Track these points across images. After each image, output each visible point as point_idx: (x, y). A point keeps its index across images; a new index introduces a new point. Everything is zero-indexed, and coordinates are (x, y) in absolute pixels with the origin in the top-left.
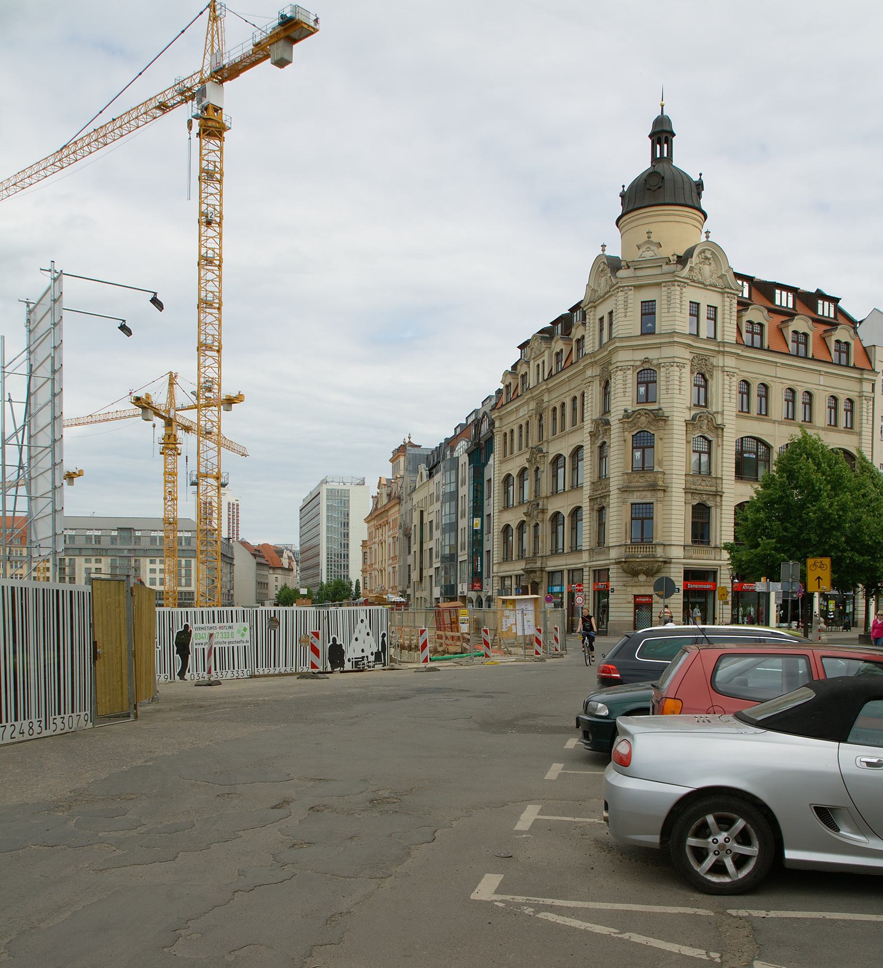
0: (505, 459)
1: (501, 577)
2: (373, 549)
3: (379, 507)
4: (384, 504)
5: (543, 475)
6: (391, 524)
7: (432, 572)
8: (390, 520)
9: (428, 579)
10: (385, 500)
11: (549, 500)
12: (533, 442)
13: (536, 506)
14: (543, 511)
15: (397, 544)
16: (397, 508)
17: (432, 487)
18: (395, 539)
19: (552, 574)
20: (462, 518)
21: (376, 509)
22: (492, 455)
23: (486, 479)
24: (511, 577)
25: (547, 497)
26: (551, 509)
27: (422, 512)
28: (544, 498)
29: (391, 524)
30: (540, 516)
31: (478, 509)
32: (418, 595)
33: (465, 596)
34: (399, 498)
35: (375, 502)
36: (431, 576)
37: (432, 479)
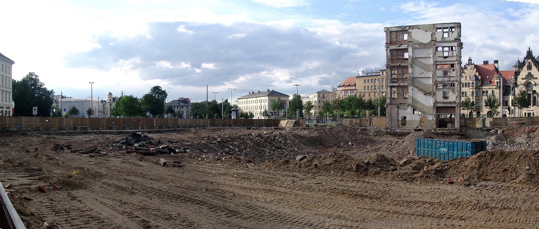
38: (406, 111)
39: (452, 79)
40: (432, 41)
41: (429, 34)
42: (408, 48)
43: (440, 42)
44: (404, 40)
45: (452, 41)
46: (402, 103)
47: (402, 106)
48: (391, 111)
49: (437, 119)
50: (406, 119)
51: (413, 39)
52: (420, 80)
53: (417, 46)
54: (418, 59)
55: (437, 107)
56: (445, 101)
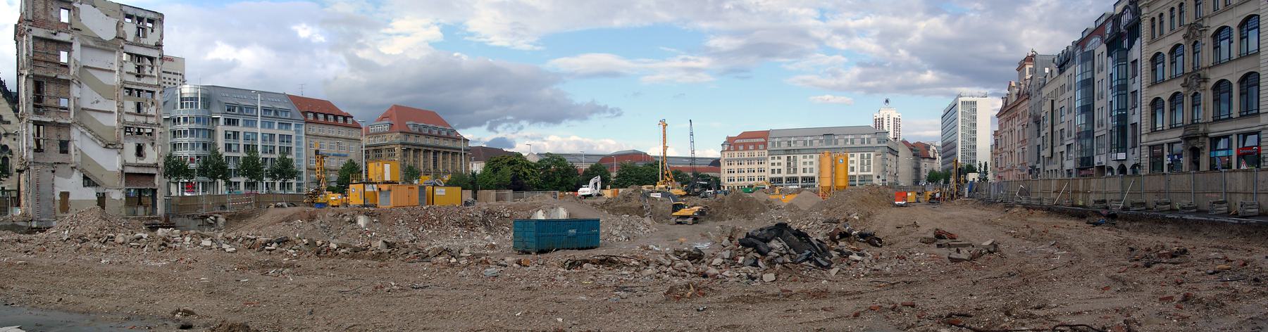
0: (1153, 39)
1: (1150, 146)
2: (1003, 137)
3: (1009, 104)
4: (1014, 101)
5: (1204, 47)
6: (1021, 115)
7: (1064, 148)
8: (1020, 112)
9: (1059, 155)
10: (1014, 98)
11: (1212, 70)
12: (1189, 18)
13: (1197, 76)
14: (1205, 80)
15: (1027, 131)
16: (1026, 102)
17: (1063, 80)
18: (1025, 127)
19: (1216, 140)
20: (1098, 99)
21: (1005, 105)
22: (1138, 42)
23: (1130, 60)
24: (1163, 144)
25: (1209, 68)
26: (1214, 77)
27: (1053, 101)
28: (1206, 68)
29: (1021, 115)
30: (1202, 85)
31: (1121, 88)
32: (1048, 168)
33: (1104, 166)
34: (1028, 94)
35: (1005, 101)
36: (1062, 153)
37: (1063, 76)
38: (69, 180)
39: (150, 120)
40: (118, 38)
41: (113, 22)
42: (71, 41)
43: (132, 44)
44: (62, 21)
45: (151, 48)
46: (60, 161)
47: (60, 169)
48: (38, 179)
49: (127, 197)
50: (71, 198)
51: (82, 25)
52: (93, 115)
53: (91, 44)
54: (89, 70)
55: (127, 174)
56: (140, 162)
